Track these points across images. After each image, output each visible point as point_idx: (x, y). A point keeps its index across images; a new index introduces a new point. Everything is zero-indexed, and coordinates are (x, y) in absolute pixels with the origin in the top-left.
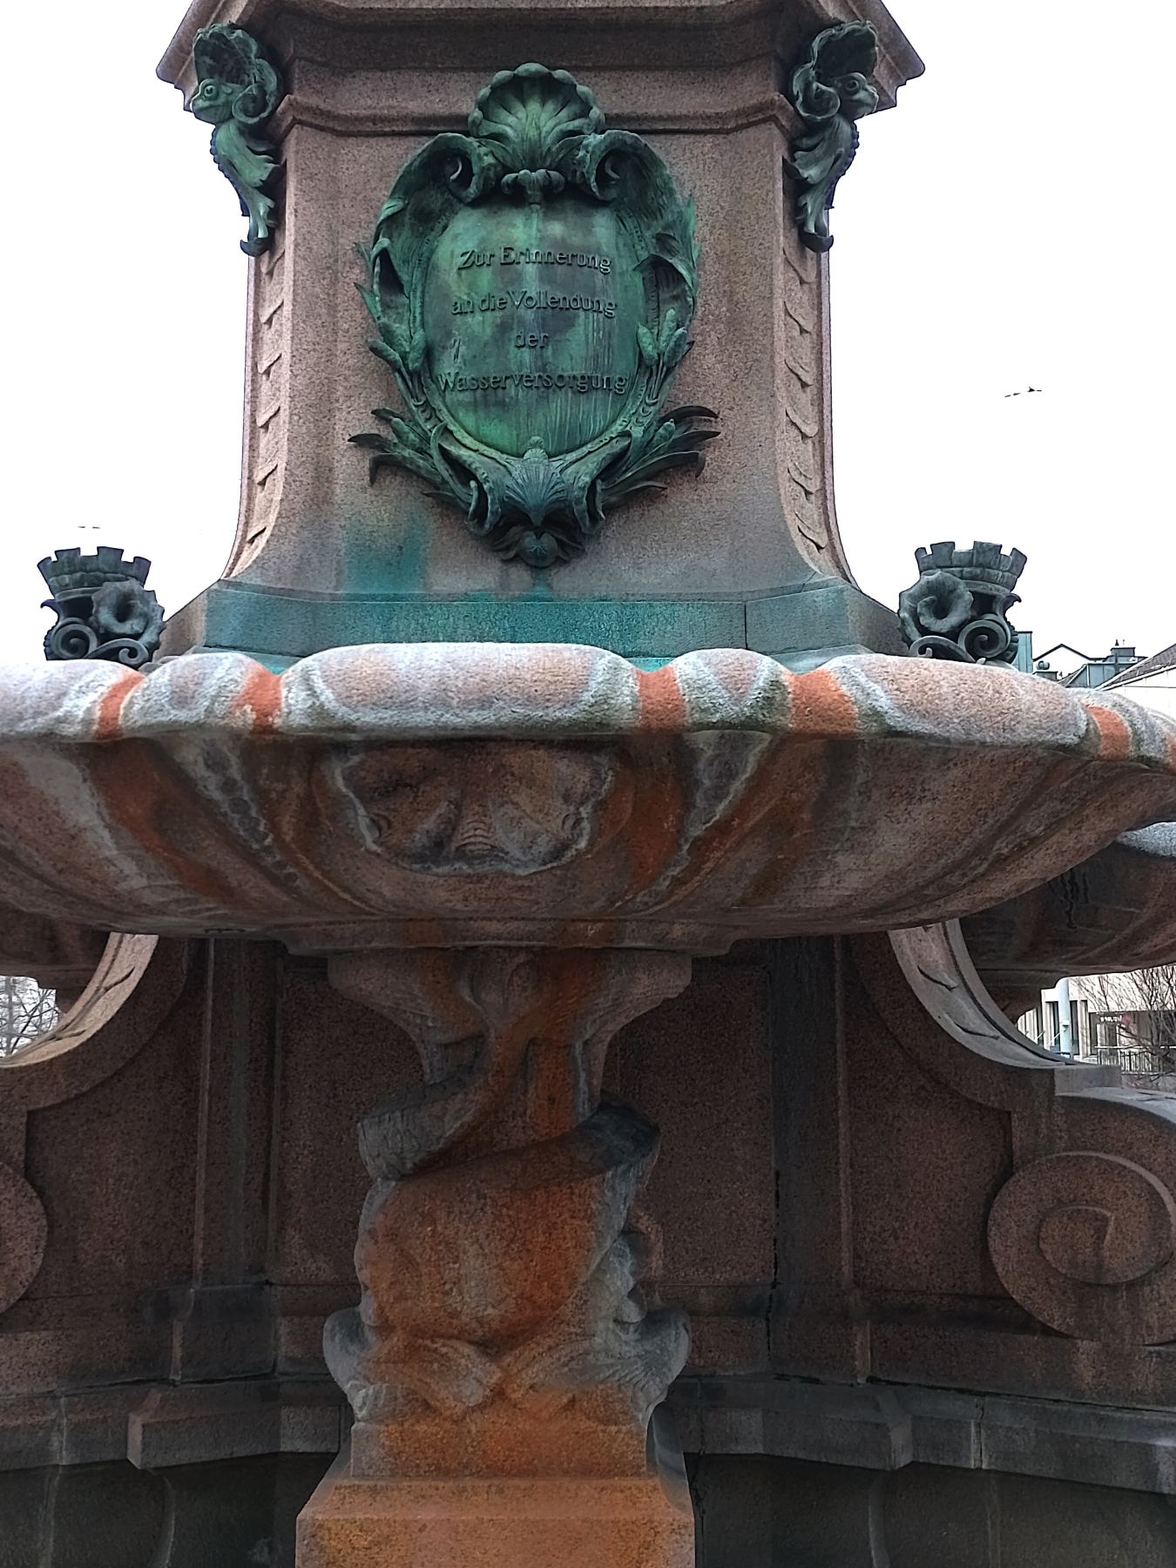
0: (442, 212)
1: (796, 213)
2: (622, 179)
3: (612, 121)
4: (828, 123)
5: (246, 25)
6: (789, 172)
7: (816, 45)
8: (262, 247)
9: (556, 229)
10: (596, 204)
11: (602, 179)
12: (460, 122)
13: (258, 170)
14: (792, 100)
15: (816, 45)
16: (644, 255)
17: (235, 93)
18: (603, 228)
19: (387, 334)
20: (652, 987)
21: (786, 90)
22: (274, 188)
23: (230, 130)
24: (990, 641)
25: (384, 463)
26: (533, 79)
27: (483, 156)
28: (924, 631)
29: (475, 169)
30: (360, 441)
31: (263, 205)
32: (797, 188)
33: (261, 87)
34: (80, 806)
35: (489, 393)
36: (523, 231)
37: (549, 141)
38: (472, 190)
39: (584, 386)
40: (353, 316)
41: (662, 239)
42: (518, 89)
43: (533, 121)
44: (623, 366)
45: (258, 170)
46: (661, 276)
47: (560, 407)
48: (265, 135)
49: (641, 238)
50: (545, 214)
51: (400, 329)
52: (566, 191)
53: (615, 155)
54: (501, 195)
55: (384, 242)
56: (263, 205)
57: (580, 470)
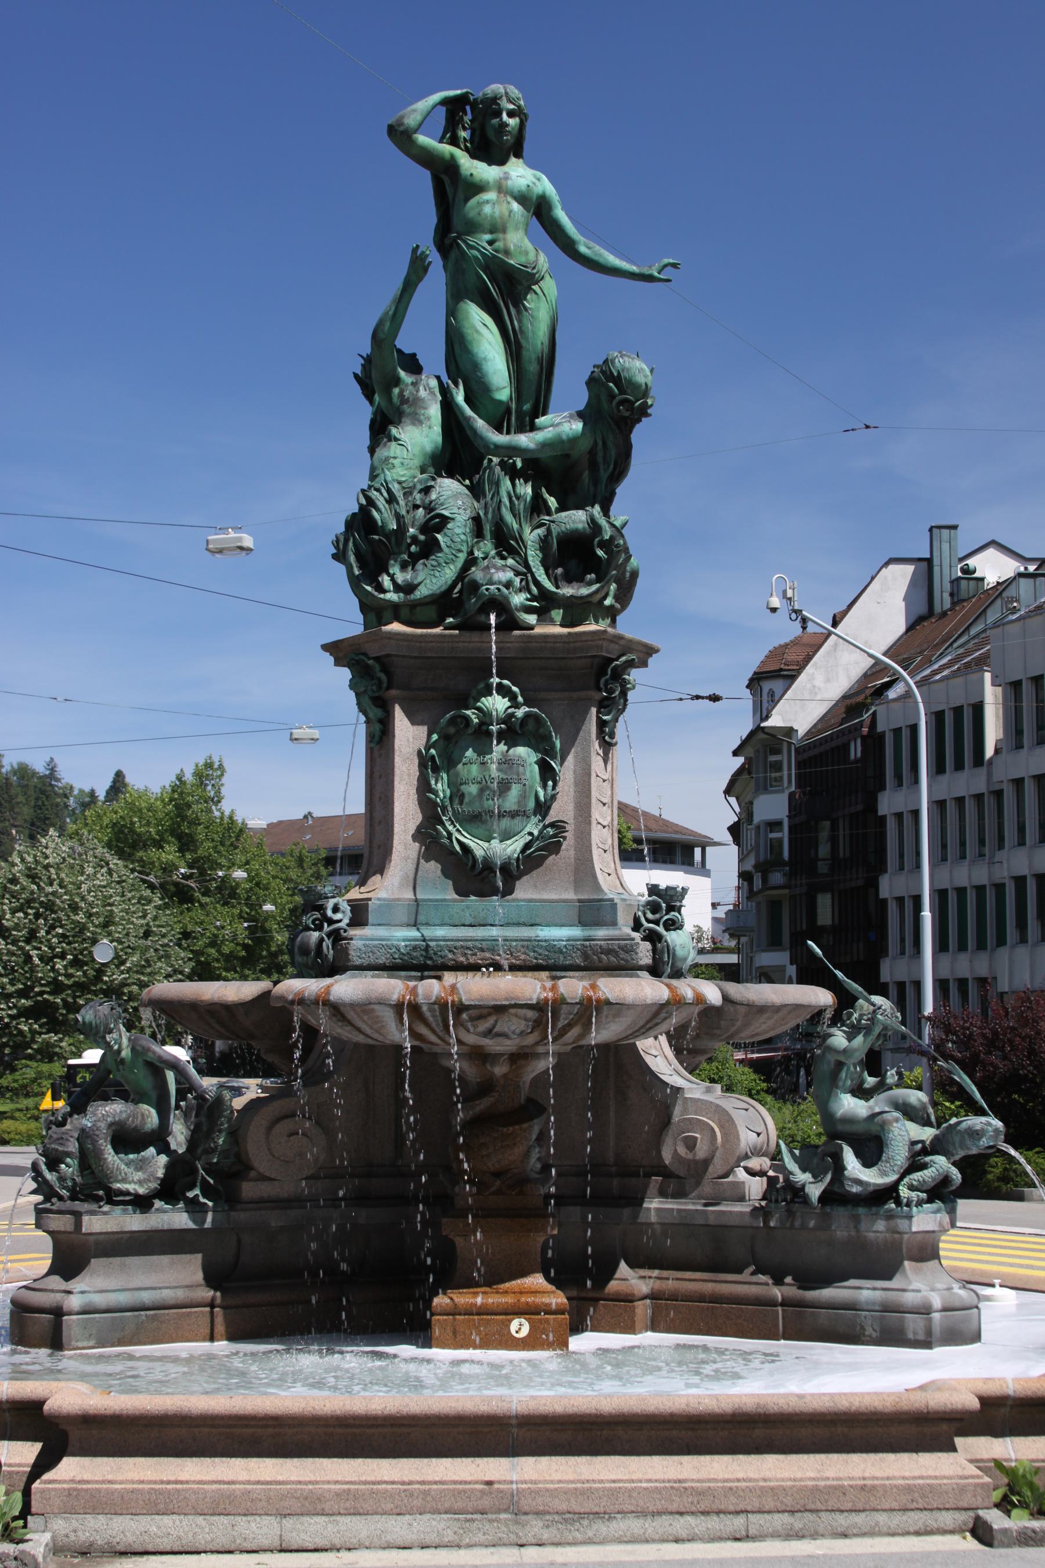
28: (648, 921)
39: (513, 815)
44: (531, 804)
57: (513, 847)
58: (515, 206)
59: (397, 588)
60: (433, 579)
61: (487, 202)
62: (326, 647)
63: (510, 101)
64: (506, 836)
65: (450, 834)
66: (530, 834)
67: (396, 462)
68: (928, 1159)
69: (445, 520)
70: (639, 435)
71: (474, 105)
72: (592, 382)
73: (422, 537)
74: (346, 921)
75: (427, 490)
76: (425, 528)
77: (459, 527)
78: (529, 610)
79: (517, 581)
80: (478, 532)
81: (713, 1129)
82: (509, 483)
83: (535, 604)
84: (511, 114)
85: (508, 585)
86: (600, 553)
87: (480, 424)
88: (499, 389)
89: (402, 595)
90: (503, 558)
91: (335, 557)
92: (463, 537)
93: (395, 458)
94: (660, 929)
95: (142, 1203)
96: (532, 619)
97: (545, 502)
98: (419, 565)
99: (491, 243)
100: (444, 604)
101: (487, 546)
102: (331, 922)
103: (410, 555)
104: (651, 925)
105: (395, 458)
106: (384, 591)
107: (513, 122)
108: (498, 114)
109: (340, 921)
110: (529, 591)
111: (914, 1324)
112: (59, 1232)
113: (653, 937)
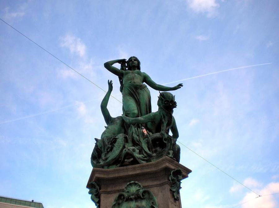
0: (122, 203)
1: (173, 196)
2: (145, 195)
3: (144, 187)
4: (175, 183)
6: (171, 190)
7: (171, 173)
9: (137, 204)
10: (142, 199)
11: (143, 195)
12: (123, 191)
13: (97, 200)
14: (170, 180)
15: (171, 173)
16: (150, 205)
17: (94, 190)
18: (144, 203)
23: (93, 196)
27: (126, 195)
29: (125, 197)
31: (98, 204)
32: (172, 193)
33: (97, 189)
37: (135, 192)
41: (153, 203)
42: (131, 184)
43: (133, 189)
45: (97, 200)
49: (150, 203)
50: (136, 202)
52: (138, 198)
53: (145, 192)
54: (129, 200)
56: (98, 204)
58: (136, 75)
72: (159, 104)
73: (110, 146)
84: (135, 60)
86: (165, 142)
88: (134, 110)
92: (121, 142)
99: (130, 82)
100: (117, 161)
107: (136, 62)
108: (131, 60)
110: (143, 155)
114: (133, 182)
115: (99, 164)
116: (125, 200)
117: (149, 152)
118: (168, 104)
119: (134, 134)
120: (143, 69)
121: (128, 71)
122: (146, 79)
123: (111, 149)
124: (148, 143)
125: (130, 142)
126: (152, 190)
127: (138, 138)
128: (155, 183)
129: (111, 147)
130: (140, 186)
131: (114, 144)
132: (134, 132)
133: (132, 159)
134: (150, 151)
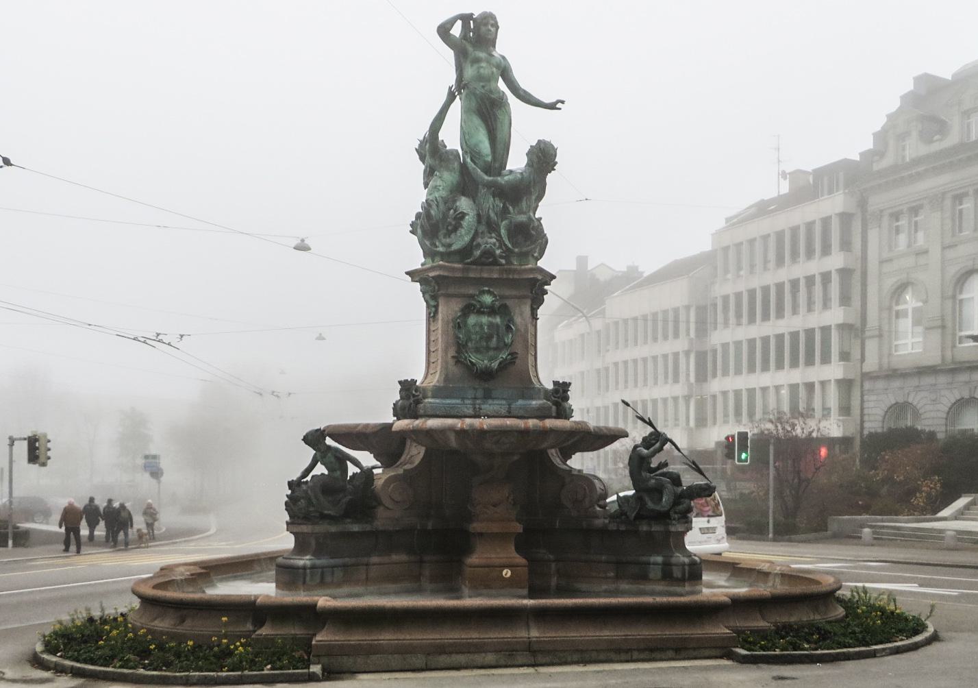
2: (501, 310)
5: (433, 277)
8: (432, 316)
9: (490, 319)
10: (498, 314)
12: (472, 296)
13: (433, 303)
16: (505, 323)
18: (498, 320)
19: (458, 338)
20: (516, 458)
21: (532, 293)
22: (436, 307)
24: (564, 413)
25: (458, 360)
26: (487, 291)
28: (555, 397)
30: (453, 357)
31: (433, 309)
33: (434, 288)
34: (452, 437)
35: (477, 350)
36: (485, 320)
38: (475, 311)
40: (451, 332)
46: (508, 328)
47: (491, 353)
48: (434, 298)
51: (461, 336)
52: (492, 311)
55: (458, 320)
56: (433, 309)
57: (495, 365)
58: (494, 70)
59: (443, 245)
60: (460, 240)
61: (482, 67)
62: (407, 273)
63: (492, 20)
64: (492, 359)
65: (466, 358)
66: (502, 357)
67: (441, 188)
68: (682, 500)
69: (463, 215)
70: (550, 178)
71: (475, 20)
74: (421, 396)
75: (455, 201)
76: (455, 218)
77: (470, 219)
78: (501, 257)
79: (497, 244)
80: (479, 221)
81: (585, 489)
82: (492, 199)
83: (504, 254)
84: (492, 25)
85: (494, 244)
86: (533, 232)
87: (479, 170)
89: (445, 249)
90: (491, 234)
91: (411, 232)
93: (440, 186)
94: (560, 400)
95: (332, 519)
96: (503, 261)
97: (508, 208)
98: (453, 236)
99: (483, 87)
100: (465, 252)
101: (482, 228)
102: (414, 396)
103: (447, 229)
104: (556, 399)
105: (440, 186)
106: (437, 247)
107: (493, 29)
109: (418, 396)
111: (677, 573)
112: (298, 533)
113: (557, 404)
114: (487, 289)
115: (435, 249)
116: (475, 311)
117: (510, 246)
118: (543, 158)
119: (490, 211)
120: (502, 47)
121: (473, 39)
122: (505, 72)
123: (455, 229)
124: (509, 231)
125: (484, 223)
126: (509, 303)
127: (496, 219)
128: (514, 293)
129: (455, 224)
130: (495, 296)
131: (462, 222)
132: (491, 207)
133: (491, 260)
134: (510, 242)
